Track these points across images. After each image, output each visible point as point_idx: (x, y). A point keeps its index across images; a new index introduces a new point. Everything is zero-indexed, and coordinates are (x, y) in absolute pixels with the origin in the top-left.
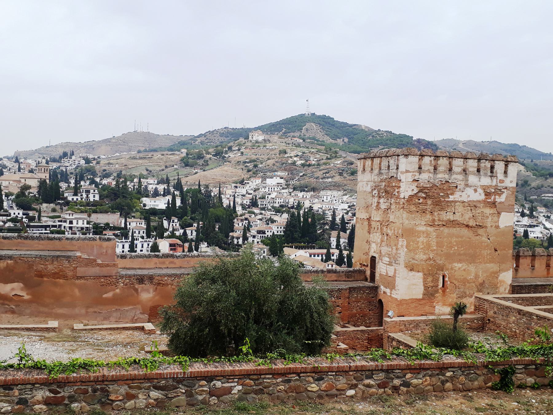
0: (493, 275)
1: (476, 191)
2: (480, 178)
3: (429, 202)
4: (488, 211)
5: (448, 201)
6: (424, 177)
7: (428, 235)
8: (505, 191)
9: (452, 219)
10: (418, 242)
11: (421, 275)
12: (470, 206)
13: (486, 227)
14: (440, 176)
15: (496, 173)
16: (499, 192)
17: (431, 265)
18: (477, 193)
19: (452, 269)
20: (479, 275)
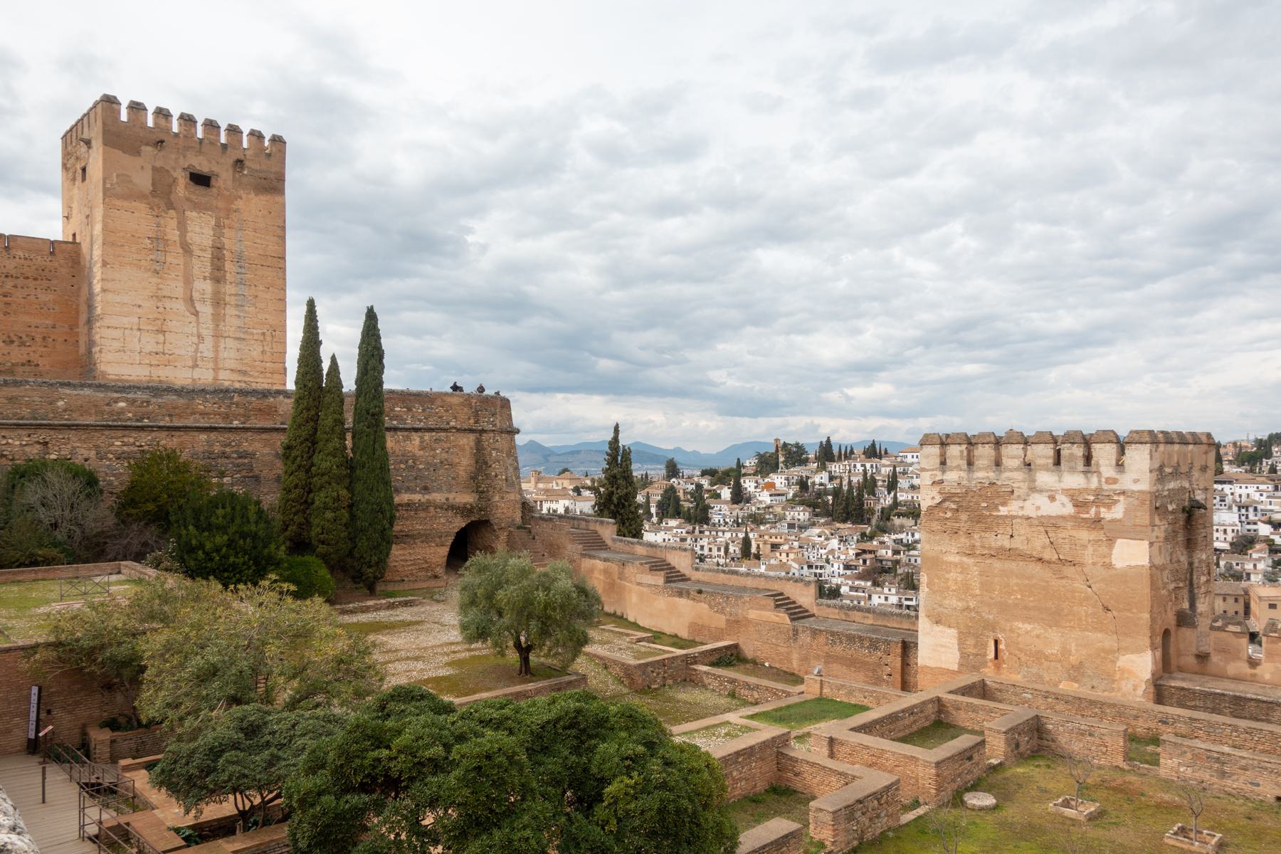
0: (1103, 654)
1: (1052, 498)
2: (1060, 477)
3: (964, 516)
4: (1084, 535)
5: (998, 516)
6: (952, 476)
7: (964, 569)
8: (1122, 498)
9: (1008, 547)
10: (948, 579)
11: (953, 632)
12: (1042, 524)
13: (1082, 565)
14: (980, 475)
15: (1098, 465)
16: (1107, 501)
17: (972, 619)
18: (1057, 503)
19: (1012, 630)
20: (1070, 651)
